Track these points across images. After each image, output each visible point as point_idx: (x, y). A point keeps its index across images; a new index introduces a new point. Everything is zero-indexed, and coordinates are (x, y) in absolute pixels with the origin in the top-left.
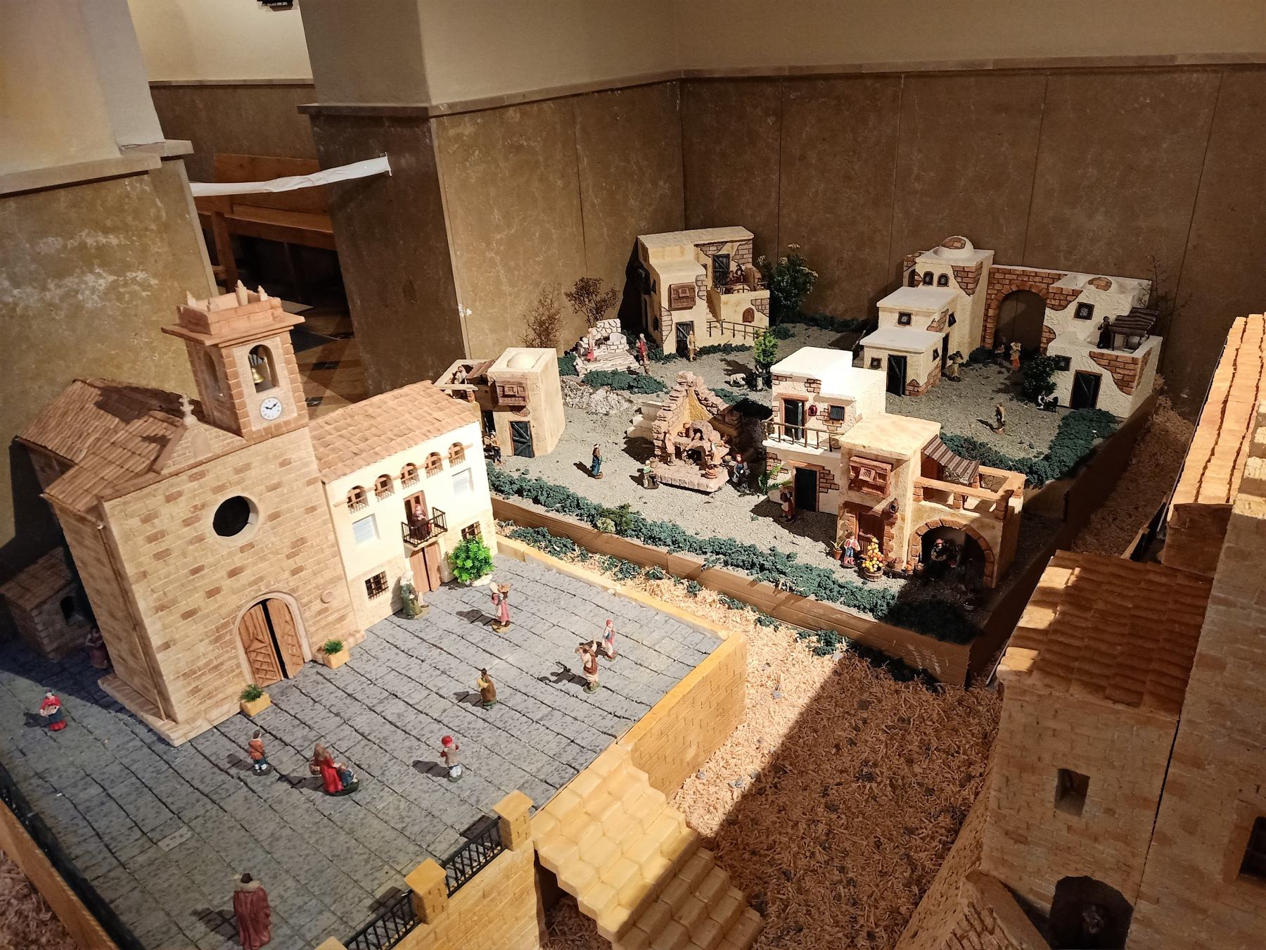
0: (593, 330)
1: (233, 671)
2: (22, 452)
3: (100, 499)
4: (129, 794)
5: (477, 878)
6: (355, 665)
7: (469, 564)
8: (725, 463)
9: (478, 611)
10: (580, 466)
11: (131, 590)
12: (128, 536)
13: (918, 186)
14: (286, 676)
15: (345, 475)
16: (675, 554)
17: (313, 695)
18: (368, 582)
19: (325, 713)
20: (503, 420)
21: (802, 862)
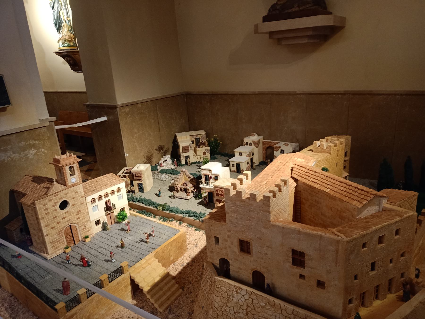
0: (163, 159)
1: (62, 242)
2: (13, 193)
3: (34, 201)
4: (37, 270)
5: (116, 280)
6: (92, 241)
7: (121, 217)
8: (192, 192)
9: (123, 229)
10: (156, 194)
11: (40, 222)
12: (40, 209)
14: (75, 244)
15: (90, 195)
16: (176, 215)
17: (82, 248)
18: (96, 222)
19: (84, 251)
20: (136, 183)
21: (194, 280)
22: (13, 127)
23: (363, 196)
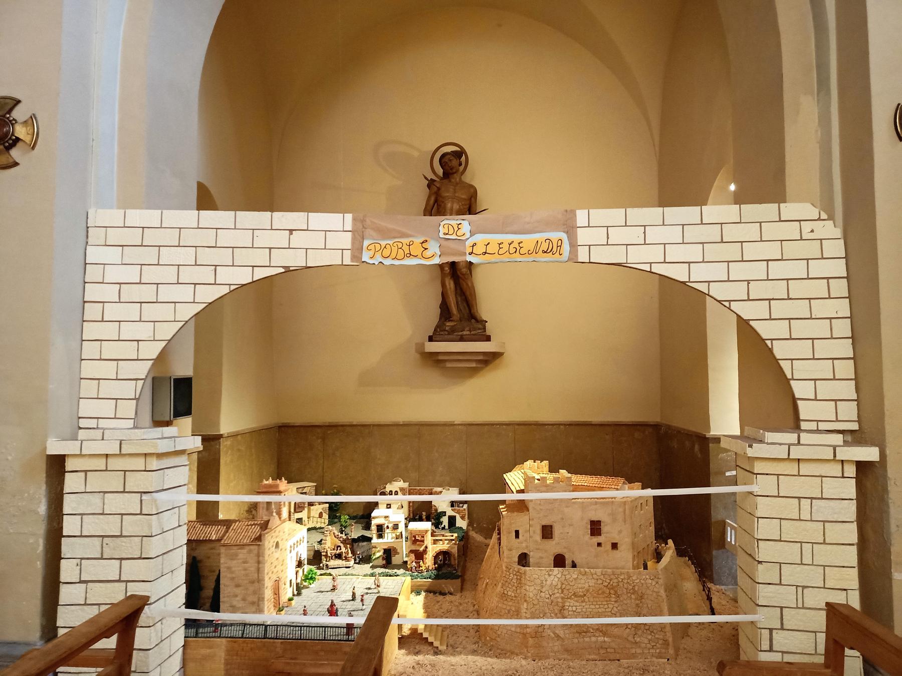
13: (380, 462)
23: (616, 482)
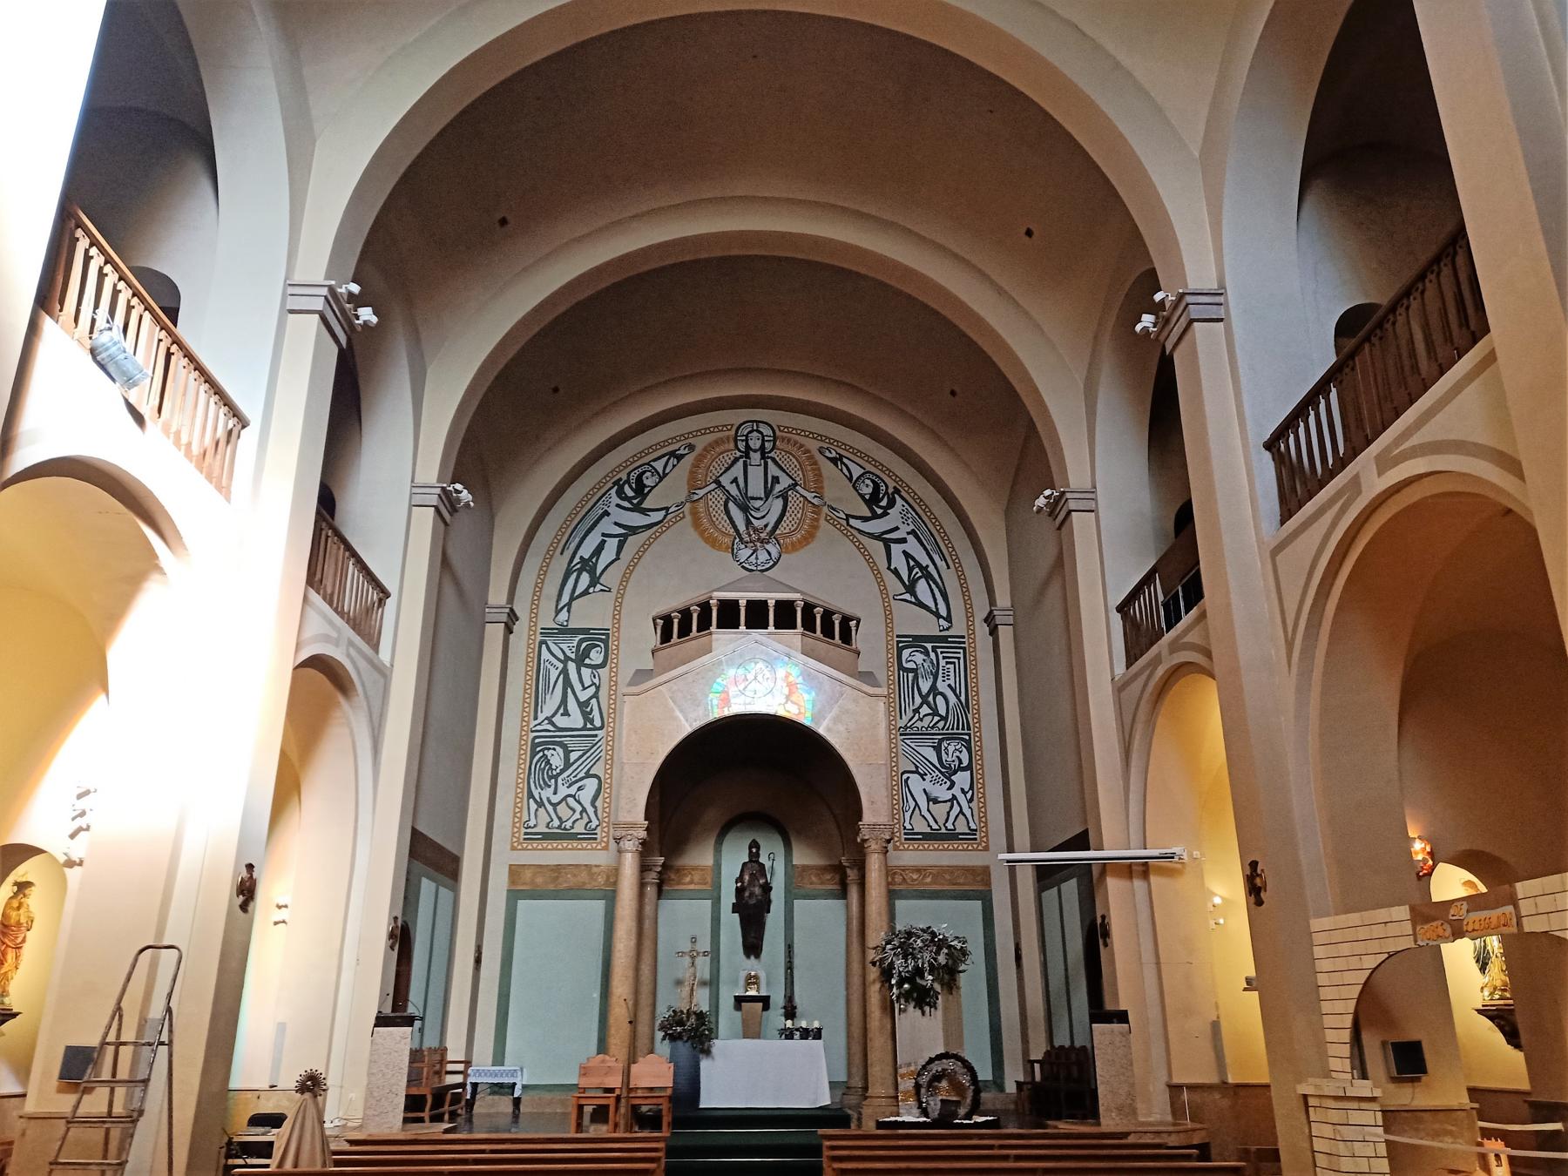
22: (1431, 1104)
